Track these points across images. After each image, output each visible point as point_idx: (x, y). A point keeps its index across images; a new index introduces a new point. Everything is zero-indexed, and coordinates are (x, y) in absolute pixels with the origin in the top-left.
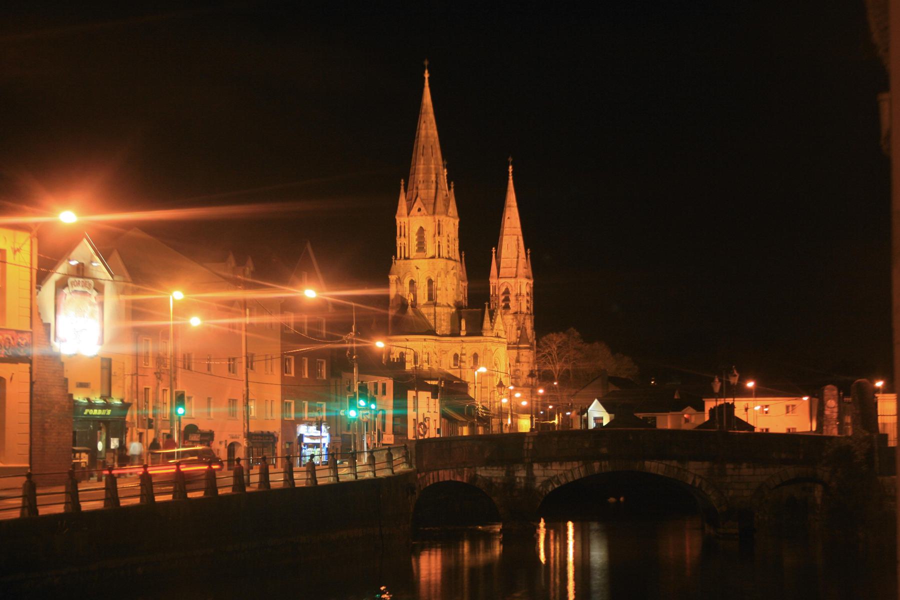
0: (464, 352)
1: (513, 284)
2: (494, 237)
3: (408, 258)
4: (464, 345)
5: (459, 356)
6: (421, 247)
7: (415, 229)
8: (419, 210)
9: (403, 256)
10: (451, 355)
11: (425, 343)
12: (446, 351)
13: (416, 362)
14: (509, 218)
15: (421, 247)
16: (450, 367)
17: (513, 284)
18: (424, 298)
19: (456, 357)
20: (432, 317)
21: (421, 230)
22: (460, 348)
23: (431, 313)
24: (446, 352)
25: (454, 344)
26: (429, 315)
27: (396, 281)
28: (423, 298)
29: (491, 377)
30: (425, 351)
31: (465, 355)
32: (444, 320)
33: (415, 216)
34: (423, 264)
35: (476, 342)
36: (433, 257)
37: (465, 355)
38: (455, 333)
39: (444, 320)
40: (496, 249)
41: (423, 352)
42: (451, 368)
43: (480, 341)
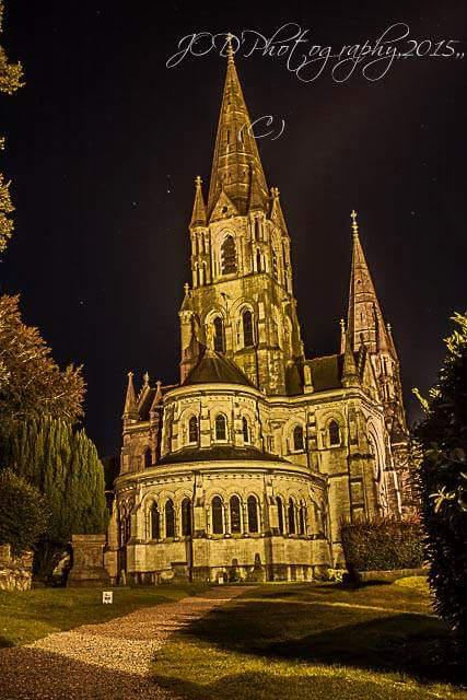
0: (312, 419)
2: (341, 306)
3: (211, 284)
4: (312, 408)
5: (304, 429)
6: (230, 265)
7: (219, 241)
8: (225, 210)
9: (201, 282)
10: (288, 428)
11: (236, 399)
12: (279, 423)
13: (221, 435)
14: (359, 282)
15: (230, 265)
16: (289, 451)
19: (298, 432)
20: (253, 369)
21: (229, 245)
22: (304, 415)
24: (280, 425)
25: (293, 410)
27: (191, 320)
28: (235, 339)
31: (314, 424)
32: (273, 372)
33: (218, 220)
34: (234, 288)
35: (333, 399)
36: (252, 274)
37: (314, 424)
38: (293, 386)
40: (346, 321)
41: (233, 413)
42: (289, 454)
43: (339, 398)
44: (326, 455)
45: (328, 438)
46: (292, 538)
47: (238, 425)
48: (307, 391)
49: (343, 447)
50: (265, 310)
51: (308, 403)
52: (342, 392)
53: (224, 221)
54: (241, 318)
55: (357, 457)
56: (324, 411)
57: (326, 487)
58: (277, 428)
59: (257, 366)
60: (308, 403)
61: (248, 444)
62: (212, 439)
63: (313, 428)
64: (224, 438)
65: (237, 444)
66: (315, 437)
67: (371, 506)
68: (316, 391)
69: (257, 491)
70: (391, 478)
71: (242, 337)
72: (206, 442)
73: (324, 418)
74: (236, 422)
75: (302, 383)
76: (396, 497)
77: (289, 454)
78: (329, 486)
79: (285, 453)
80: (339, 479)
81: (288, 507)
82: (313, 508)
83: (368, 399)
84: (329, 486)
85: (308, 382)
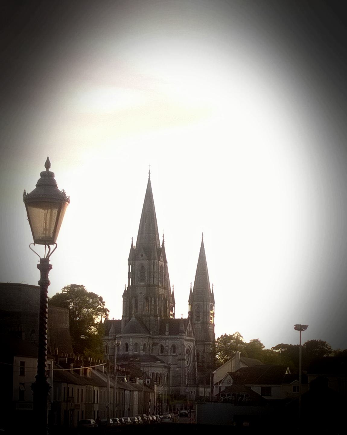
0: (167, 344)
20: (148, 323)
29: (183, 361)
30: (141, 343)
31: (167, 347)
35: (175, 339)
44: (171, 357)
45: (172, 351)
48: (167, 333)
49: (177, 356)
51: (167, 339)
52: (178, 337)
55: (180, 360)
57: (169, 368)
60: (167, 339)
61: (144, 353)
62: (133, 352)
64: (137, 351)
68: (170, 334)
70: (195, 364)
72: (131, 353)
74: (141, 347)
75: (165, 331)
77: (159, 355)
78: (170, 368)
79: (157, 354)
82: (163, 377)
83: (188, 338)
84: (170, 368)
85: (167, 330)
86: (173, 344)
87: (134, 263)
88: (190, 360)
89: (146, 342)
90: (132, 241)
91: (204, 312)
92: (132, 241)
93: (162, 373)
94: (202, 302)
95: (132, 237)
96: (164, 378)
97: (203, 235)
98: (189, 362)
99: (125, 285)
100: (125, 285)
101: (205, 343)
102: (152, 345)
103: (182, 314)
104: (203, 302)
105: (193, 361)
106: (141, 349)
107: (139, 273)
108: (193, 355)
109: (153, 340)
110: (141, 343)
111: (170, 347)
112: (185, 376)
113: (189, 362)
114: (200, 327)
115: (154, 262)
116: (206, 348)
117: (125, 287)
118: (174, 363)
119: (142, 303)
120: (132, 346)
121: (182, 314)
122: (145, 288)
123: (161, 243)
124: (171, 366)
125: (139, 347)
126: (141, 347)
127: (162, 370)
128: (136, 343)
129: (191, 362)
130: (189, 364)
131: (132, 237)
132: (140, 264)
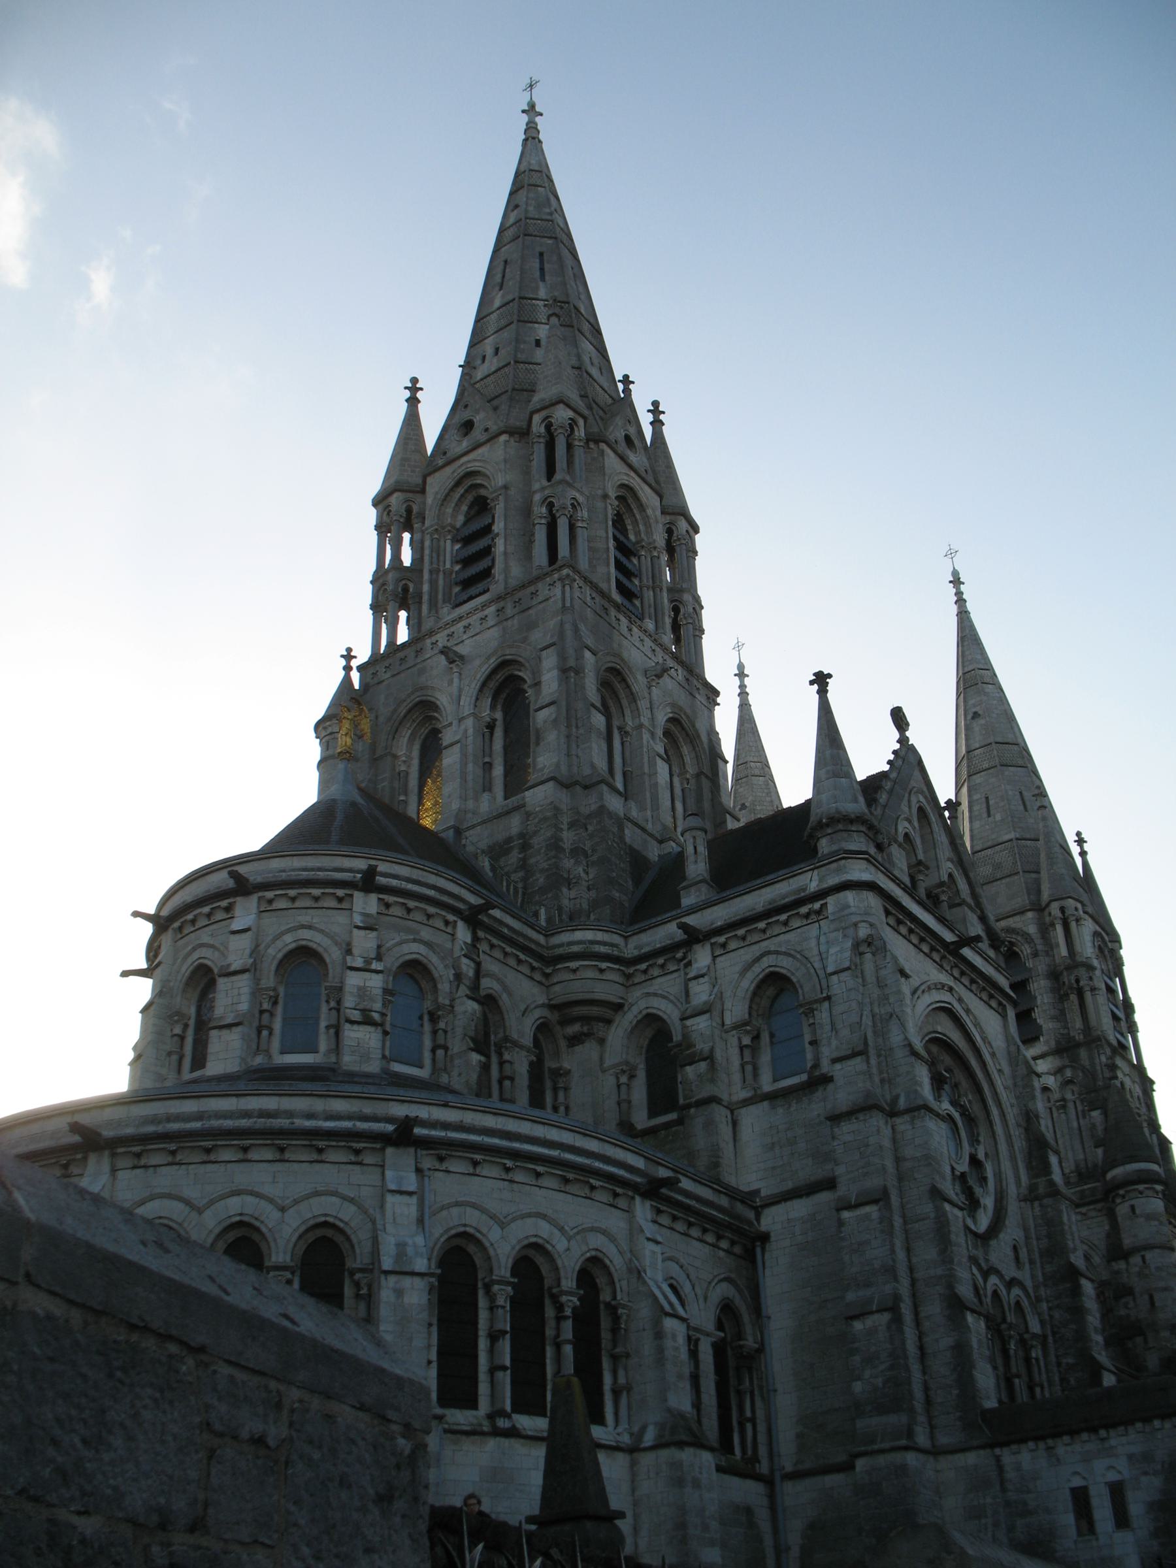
0: (701, 993)
1: (1032, 929)
4: (702, 957)
12: (586, 1019)
17: (1032, 929)
18: (487, 787)
23: (509, 840)
26: (498, 851)
32: (577, 852)
39: (577, 852)
41: (349, 952)
44: (753, 1120)
46: (513, 1433)
47: (362, 991)
50: (564, 671)
52: (811, 881)
53: (465, 459)
54: (499, 715)
56: (747, 954)
58: (575, 1041)
59: (525, 847)
60: (694, 937)
63: (701, 1024)
65: (348, 1061)
66: (710, 1058)
67: (934, 1309)
69: (346, 1214)
70: (1052, 1229)
71: (498, 771)
73: (748, 983)
74: (353, 980)
76: (1076, 1291)
78: (765, 1238)
80: (799, 1208)
81: (503, 1295)
82: (644, 1311)
84: (765, 1238)
86: (758, 970)
87: (415, 508)
88: (998, 1176)
89: (428, 944)
90: (413, 402)
91: (1054, 975)
92: (413, 402)
93: (617, 1262)
94: (1030, 915)
95: (414, 381)
96: (659, 1335)
97: (956, 581)
98: (988, 1201)
99: (348, 656)
100: (348, 656)
101: (1109, 1176)
102: (543, 1028)
103: (821, 680)
104: (1040, 909)
105: (1031, 1196)
106: (349, 1001)
107: (451, 548)
108: (1016, 1132)
109: (546, 981)
110: (365, 943)
111: (736, 1010)
112: (956, 1306)
113: (988, 1201)
114: (1050, 1081)
115: (549, 427)
116: (1122, 1210)
117: (348, 668)
118: (807, 1171)
119: (470, 722)
120: (243, 983)
121: (821, 680)
122: (492, 609)
123: (645, 420)
124: (772, 1220)
125: (338, 991)
126: (353, 980)
127: (615, 1221)
128: (304, 955)
129: (1013, 1207)
130: (983, 1222)
131: (414, 381)
132: (458, 484)
